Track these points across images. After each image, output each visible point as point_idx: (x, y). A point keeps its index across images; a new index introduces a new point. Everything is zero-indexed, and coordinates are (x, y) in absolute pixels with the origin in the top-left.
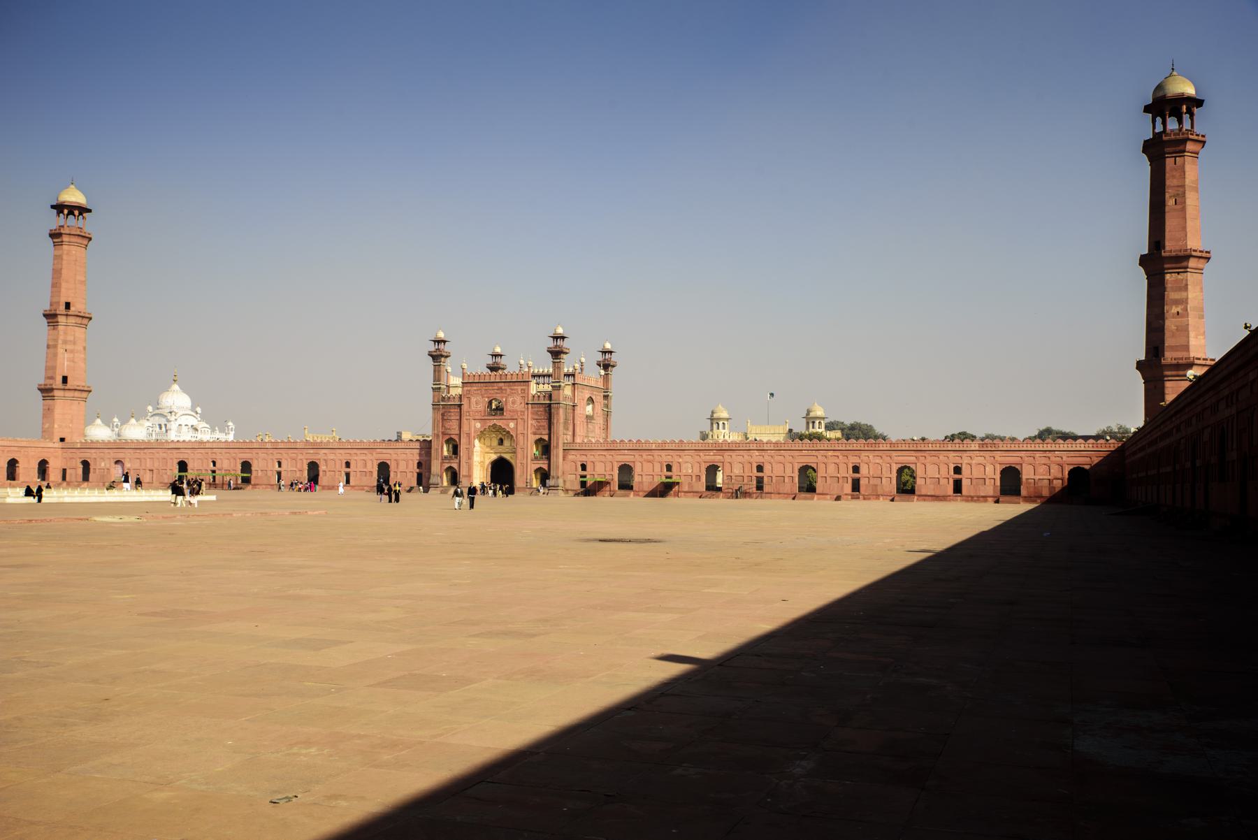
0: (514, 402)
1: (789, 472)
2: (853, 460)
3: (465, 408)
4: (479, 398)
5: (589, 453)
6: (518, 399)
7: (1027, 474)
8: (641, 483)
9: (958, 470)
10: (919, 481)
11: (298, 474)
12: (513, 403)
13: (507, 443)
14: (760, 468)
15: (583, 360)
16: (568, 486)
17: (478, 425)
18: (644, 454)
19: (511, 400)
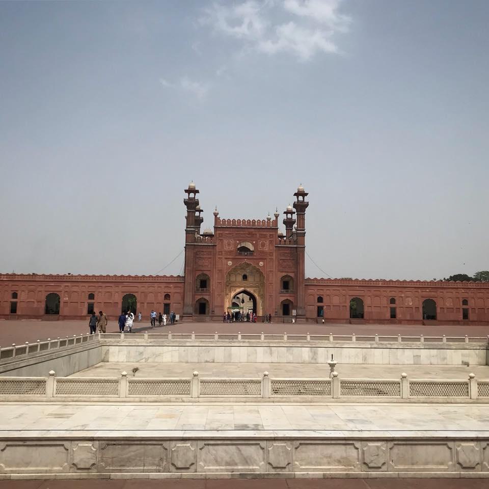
3: (218, 248)
4: (232, 242)
5: (325, 288)
6: (267, 243)
11: (35, 305)
12: (263, 245)
13: (250, 279)
14: (465, 302)
16: (308, 315)
17: (230, 263)
18: (373, 290)
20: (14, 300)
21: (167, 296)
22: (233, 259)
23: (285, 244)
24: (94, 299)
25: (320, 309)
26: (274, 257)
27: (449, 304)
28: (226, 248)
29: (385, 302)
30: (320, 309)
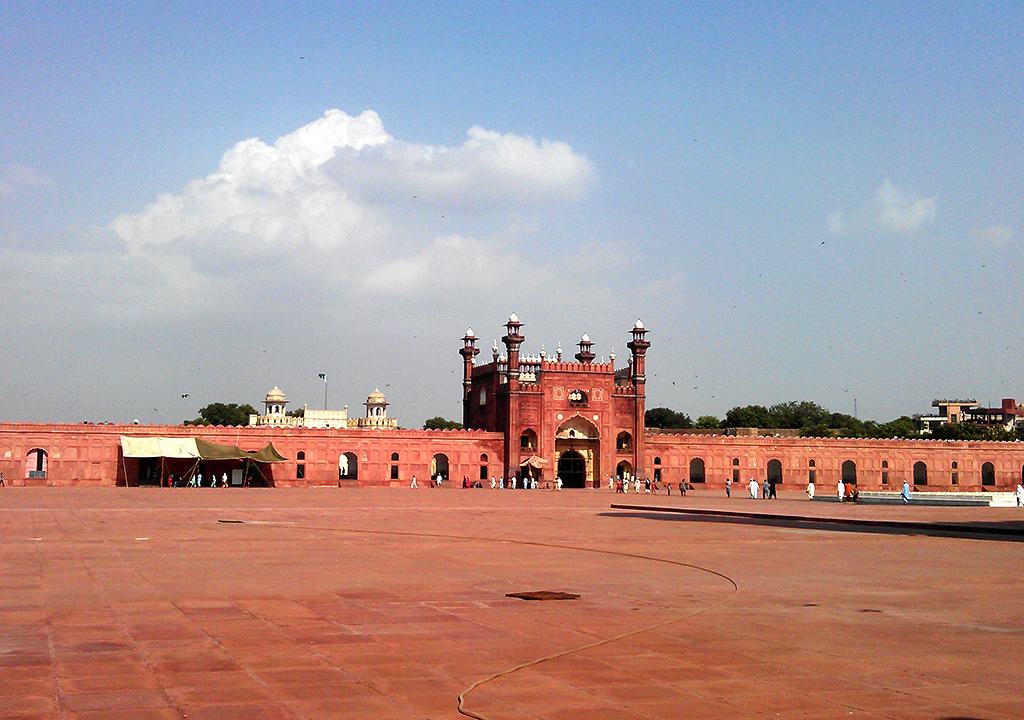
0: (599, 396)
1: (836, 466)
2: (885, 457)
3: (546, 398)
4: (561, 389)
6: (602, 392)
7: (999, 470)
8: (712, 476)
9: (955, 465)
10: (929, 474)
11: (328, 468)
12: (598, 394)
14: (812, 463)
15: (560, 351)
17: (560, 417)
19: (594, 391)
20: (301, 462)
21: (484, 457)
22: (565, 411)
23: (622, 393)
24: (398, 459)
25: (658, 472)
26: (610, 409)
27: (795, 465)
28: (556, 398)
29: (727, 462)
30: (658, 472)
